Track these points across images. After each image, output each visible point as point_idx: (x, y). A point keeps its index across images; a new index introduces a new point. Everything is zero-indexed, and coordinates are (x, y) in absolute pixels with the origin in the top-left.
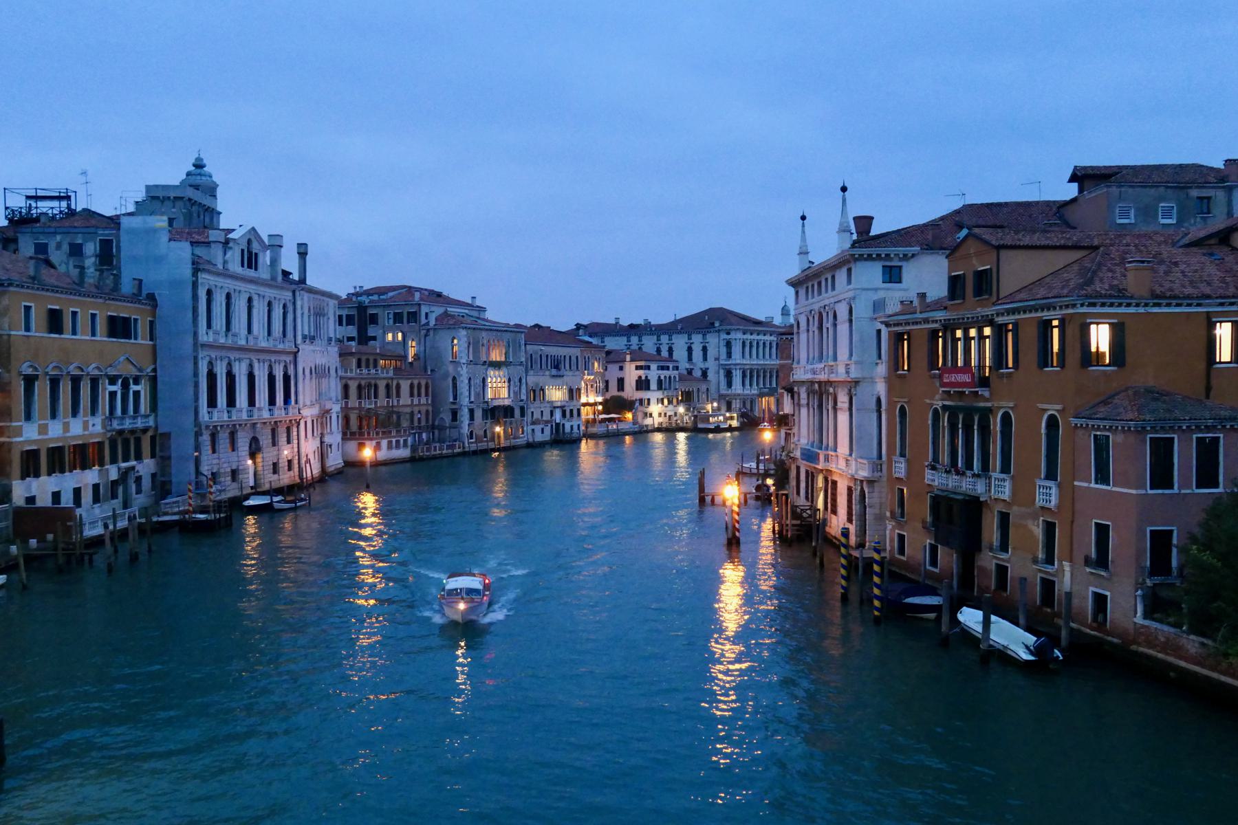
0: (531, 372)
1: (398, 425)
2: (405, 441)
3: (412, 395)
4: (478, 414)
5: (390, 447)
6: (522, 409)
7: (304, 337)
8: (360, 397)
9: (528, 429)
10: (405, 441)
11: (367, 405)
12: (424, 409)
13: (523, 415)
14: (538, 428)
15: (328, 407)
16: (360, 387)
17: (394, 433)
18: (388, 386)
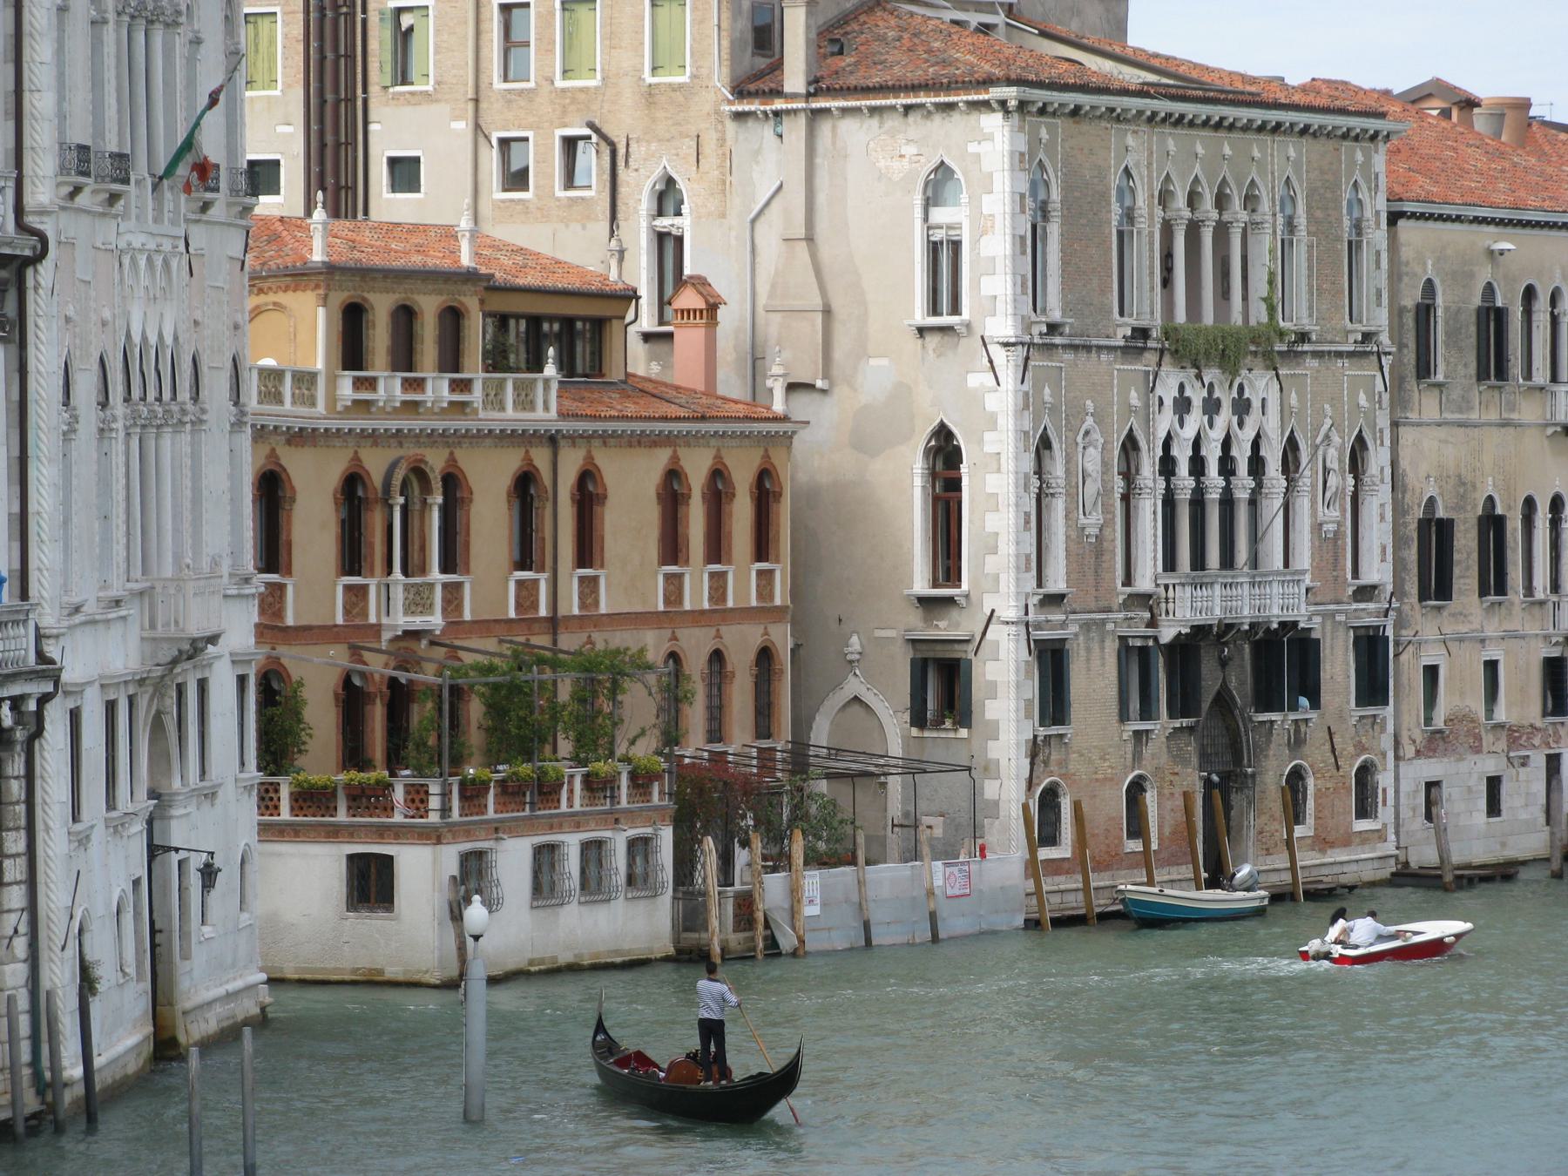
0: (1427, 406)
1: (593, 736)
2: (640, 847)
3: (672, 549)
4: (1095, 679)
5: (544, 885)
6: (1372, 652)
7: (80, 159)
8: (352, 558)
9: (1400, 783)
10: (640, 847)
11: (394, 608)
12: (741, 644)
13: (1373, 688)
14: (1463, 776)
15: (196, 627)
16: (352, 490)
17: (573, 798)
18: (525, 487)
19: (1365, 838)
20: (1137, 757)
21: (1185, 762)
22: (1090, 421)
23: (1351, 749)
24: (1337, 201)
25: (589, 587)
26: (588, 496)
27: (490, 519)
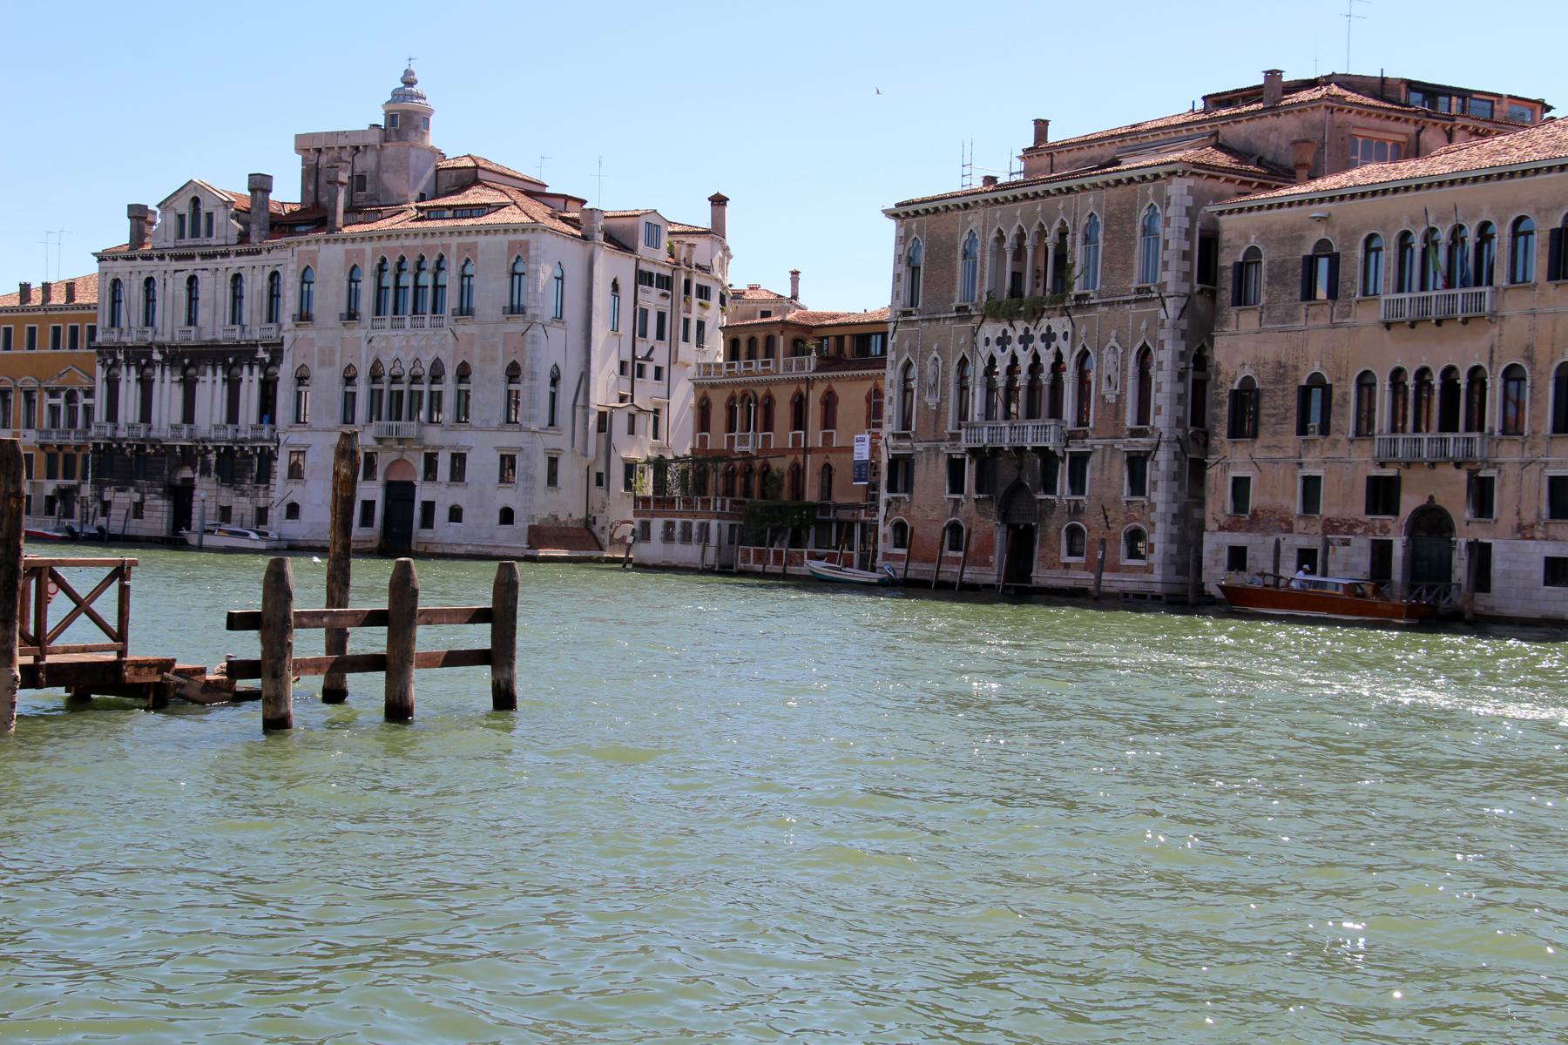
19: (1130, 569)
20: (955, 511)
21: (988, 516)
22: (935, 354)
23: (1122, 518)
24: (1132, 221)
25: (827, 438)
26: (829, 402)
27: (783, 413)
